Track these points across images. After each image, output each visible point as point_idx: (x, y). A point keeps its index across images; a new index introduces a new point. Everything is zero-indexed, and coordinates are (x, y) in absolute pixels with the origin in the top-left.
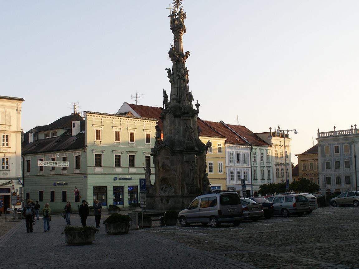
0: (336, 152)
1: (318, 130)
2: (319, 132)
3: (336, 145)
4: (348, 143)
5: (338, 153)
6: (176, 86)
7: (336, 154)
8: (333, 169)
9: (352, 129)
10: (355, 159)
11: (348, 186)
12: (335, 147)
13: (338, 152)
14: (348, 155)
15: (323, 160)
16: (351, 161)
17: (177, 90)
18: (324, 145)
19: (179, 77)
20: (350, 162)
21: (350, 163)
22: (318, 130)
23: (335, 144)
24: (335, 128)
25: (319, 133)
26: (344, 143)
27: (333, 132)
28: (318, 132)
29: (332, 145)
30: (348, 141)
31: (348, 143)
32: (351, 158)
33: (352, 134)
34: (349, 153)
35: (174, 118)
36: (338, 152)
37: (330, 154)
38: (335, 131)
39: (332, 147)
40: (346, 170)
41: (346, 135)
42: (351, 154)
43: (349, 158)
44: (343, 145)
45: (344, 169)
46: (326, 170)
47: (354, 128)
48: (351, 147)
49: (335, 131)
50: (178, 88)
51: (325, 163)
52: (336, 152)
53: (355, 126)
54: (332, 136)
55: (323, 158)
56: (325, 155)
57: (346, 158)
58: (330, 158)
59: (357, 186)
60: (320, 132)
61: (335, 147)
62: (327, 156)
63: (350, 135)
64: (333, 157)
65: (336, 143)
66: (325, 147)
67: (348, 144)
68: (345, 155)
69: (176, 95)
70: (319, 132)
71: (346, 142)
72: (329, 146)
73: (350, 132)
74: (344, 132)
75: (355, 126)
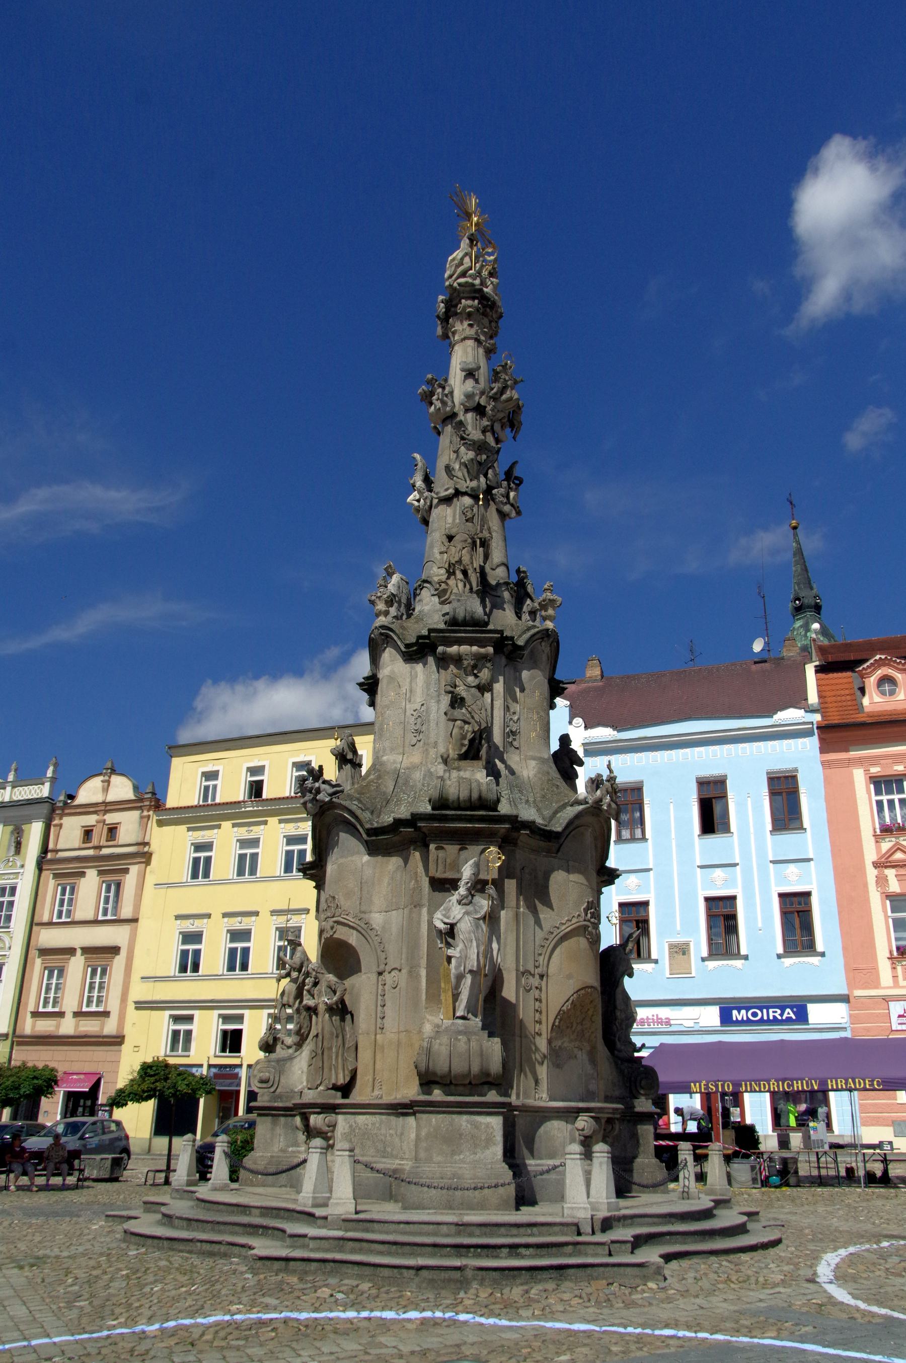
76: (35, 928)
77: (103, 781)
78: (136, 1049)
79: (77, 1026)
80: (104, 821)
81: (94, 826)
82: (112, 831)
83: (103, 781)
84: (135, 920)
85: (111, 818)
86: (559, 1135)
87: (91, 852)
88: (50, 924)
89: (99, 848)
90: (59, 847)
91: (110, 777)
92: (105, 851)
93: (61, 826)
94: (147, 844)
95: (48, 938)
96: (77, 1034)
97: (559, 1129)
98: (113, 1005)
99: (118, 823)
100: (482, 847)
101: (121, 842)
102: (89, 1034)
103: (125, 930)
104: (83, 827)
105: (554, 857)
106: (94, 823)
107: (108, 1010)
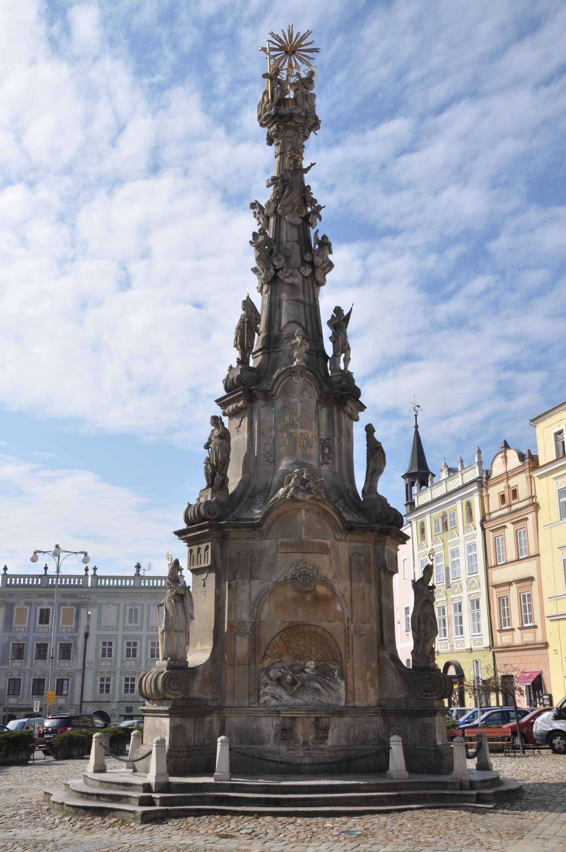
0: (41, 622)
1: (5, 569)
2: (5, 574)
3: (45, 607)
4: (72, 605)
5: (46, 626)
6: (301, 297)
7: (42, 626)
8: (29, 661)
9: (87, 575)
10: (86, 641)
11: (61, 701)
12: (42, 610)
13: (47, 622)
14: (70, 630)
15: (6, 640)
16: (76, 645)
17: (305, 315)
18: (14, 604)
19: (313, 274)
20: (73, 646)
21: (72, 649)
22: (5, 569)
23: (42, 604)
24: (46, 568)
25: (5, 576)
26: (64, 604)
27: (40, 576)
28: (3, 572)
29: (33, 607)
30: (74, 601)
31: (72, 605)
32: (75, 638)
33: (84, 586)
34: (73, 626)
35: (318, 402)
36: (47, 622)
37: (26, 625)
38: (46, 575)
39: (33, 611)
40: (62, 665)
41: (70, 586)
42: (77, 629)
43: (70, 637)
44: (62, 608)
45: (32, 662)
46: (10, 661)
47: (91, 572)
48: (78, 613)
49: (46, 575)
50: (308, 308)
51: (11, 646)
52: (41, 622)
53: (95, 569)
54: (37, 586)
55: (8, 634)
56: (14, 625)
57: (66, 638)
58: (25, 634)
59: (82, 702)
60: (8, 572)
61: (42, 610)
62: (17, 630)
63: (79, 586)
64: (34, 632)
65: (45, 601)
66: (15, 608)
67: (72, 607)
68: (64, 630)
69: (304, 325)
70: (5, 574)
71: (69, 601)
72: (25, 607)
73: (81, 580)
74: (77, 580)
75: (95, 569)
76: (490, 570)
77: (502, 458)
78: (556, 652)
79: (522, 638)
80: (509, 486)
81: (504, 491)
82: (515, 493)
83: (502, 458)
84: (538, 555)
85: (513, 482)
86: (266, 729)
87: (506, 511)
88: (496, 566)
89: (510, 506)
90: (491, 511)
91: (505, 453)
92: (514, 508)
93: (488, 496)
94: (532, 497)
95: (498, 576)
96: (523, 644)
97: (266, 725)
98: (537, 621)
99: (515, 486)
100: (205, 545)
101: (521, 499)
102: (529, 643)
103: (533, 562)
104: (499, 493)
105: (266, 539)
106: (504, 489)
107: (536, 625)
